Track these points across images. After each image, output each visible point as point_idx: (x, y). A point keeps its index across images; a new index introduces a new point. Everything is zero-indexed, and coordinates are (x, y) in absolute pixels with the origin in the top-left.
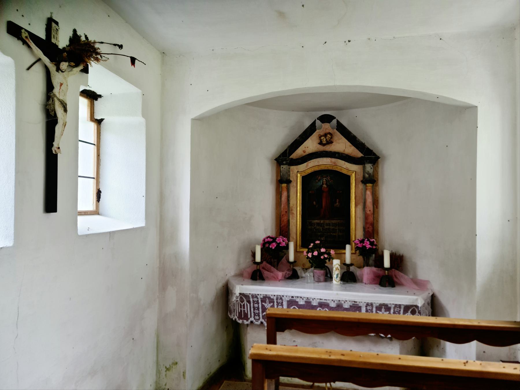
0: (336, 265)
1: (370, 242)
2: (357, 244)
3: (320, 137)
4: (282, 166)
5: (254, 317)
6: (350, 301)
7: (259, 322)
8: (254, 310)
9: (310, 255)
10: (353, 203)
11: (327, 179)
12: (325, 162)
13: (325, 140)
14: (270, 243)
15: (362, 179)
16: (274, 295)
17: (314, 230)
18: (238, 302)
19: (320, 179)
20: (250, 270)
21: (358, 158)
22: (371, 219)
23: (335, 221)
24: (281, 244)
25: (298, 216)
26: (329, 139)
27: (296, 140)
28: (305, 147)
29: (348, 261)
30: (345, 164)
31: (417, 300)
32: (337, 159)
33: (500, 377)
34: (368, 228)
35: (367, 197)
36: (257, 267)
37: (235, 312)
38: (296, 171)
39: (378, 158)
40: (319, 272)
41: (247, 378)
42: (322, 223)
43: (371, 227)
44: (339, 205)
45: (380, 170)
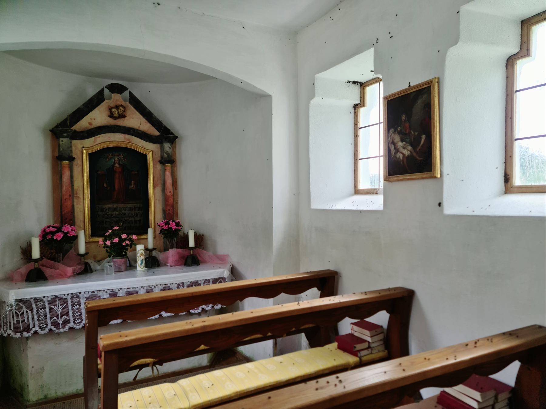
0: (140, 250)
1: (175, 222)
2: (163, 226)
3: (110, 109)
4: (61, 139)
5: (39, 326)
6: (161, 285)
7: (47, 330)
8: (38, 317)
9: (108, 243)
10: (152, 184)
11: (120, 158)
12: (117, 139)
13: (117, 112)
14: (52, 233)
15: (159, 159)
16: (68, 294)
17: (106, 216)
18: (12, 312)
19: (111, 157)
20: (24, 270)
21: (155, 136)
22: (171, 201)
23: (130, 204)
24: (69, 234)
25: (86, 200)
26: (122, 112)
27: (79, 108)
28: (91, 119)
29: (150, 246)
30: (140, 142)
31: (223, 272)
32: (132, 136)
33: (323, 309)
34: (169, 210)
35: (166, 178)
36: (34, 265)
37: (7, 325)
38: (80, 147)
39: (176, 137)
40: (120, 261)
41: (28, 403)
42: (116, 208)
43: (172, 208)
44: (134, 187)
45: (177, 151)
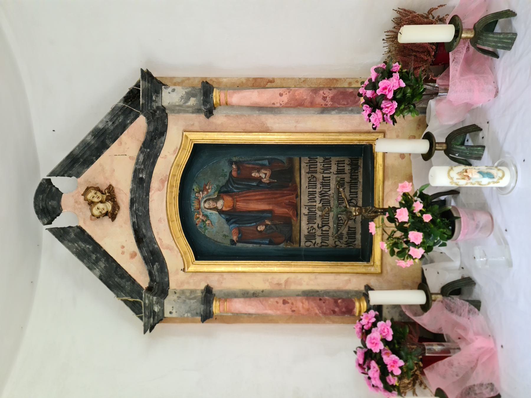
4: (167, 314)
10: (261, 137)
13: (101, 206)
17: (324, 228)
21: (149, 123)
22: (303, 93)
26: (99, 194)
28: (123, 253)
30: (166, 157)
32: (153, 175)
34: (324, 98)
43: (321, 92)
44: (265, 172)
45: (180, 74)
